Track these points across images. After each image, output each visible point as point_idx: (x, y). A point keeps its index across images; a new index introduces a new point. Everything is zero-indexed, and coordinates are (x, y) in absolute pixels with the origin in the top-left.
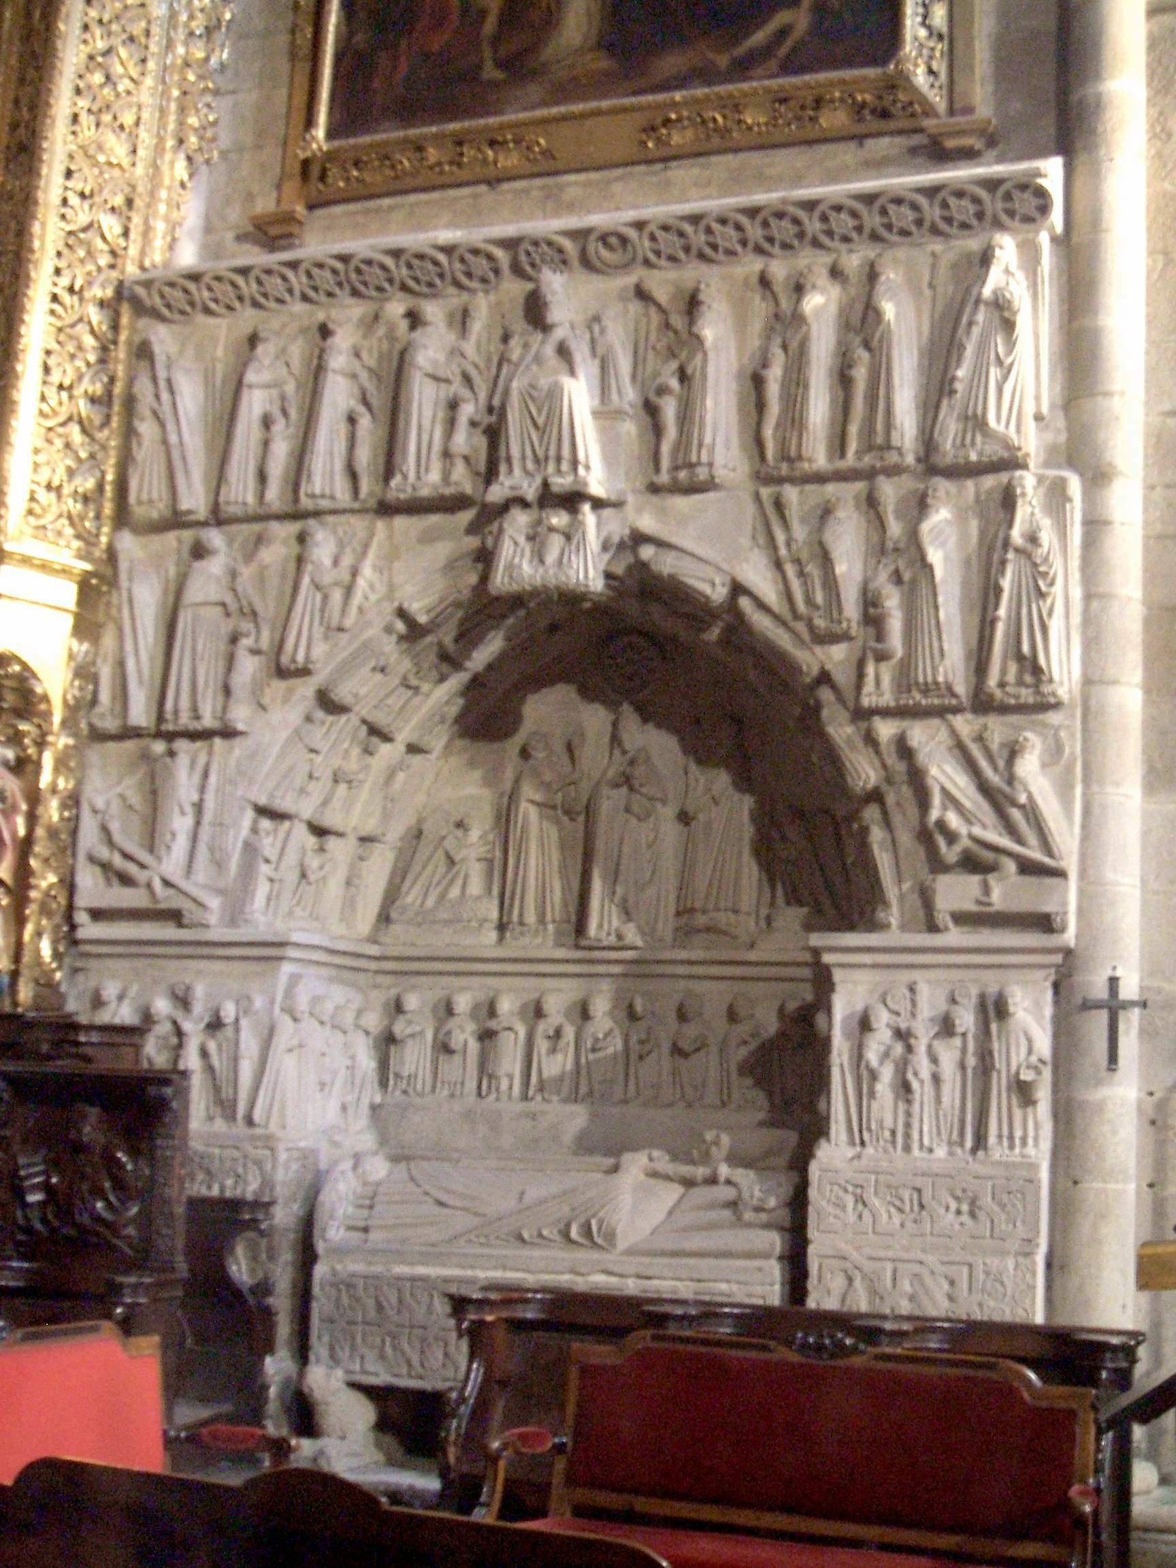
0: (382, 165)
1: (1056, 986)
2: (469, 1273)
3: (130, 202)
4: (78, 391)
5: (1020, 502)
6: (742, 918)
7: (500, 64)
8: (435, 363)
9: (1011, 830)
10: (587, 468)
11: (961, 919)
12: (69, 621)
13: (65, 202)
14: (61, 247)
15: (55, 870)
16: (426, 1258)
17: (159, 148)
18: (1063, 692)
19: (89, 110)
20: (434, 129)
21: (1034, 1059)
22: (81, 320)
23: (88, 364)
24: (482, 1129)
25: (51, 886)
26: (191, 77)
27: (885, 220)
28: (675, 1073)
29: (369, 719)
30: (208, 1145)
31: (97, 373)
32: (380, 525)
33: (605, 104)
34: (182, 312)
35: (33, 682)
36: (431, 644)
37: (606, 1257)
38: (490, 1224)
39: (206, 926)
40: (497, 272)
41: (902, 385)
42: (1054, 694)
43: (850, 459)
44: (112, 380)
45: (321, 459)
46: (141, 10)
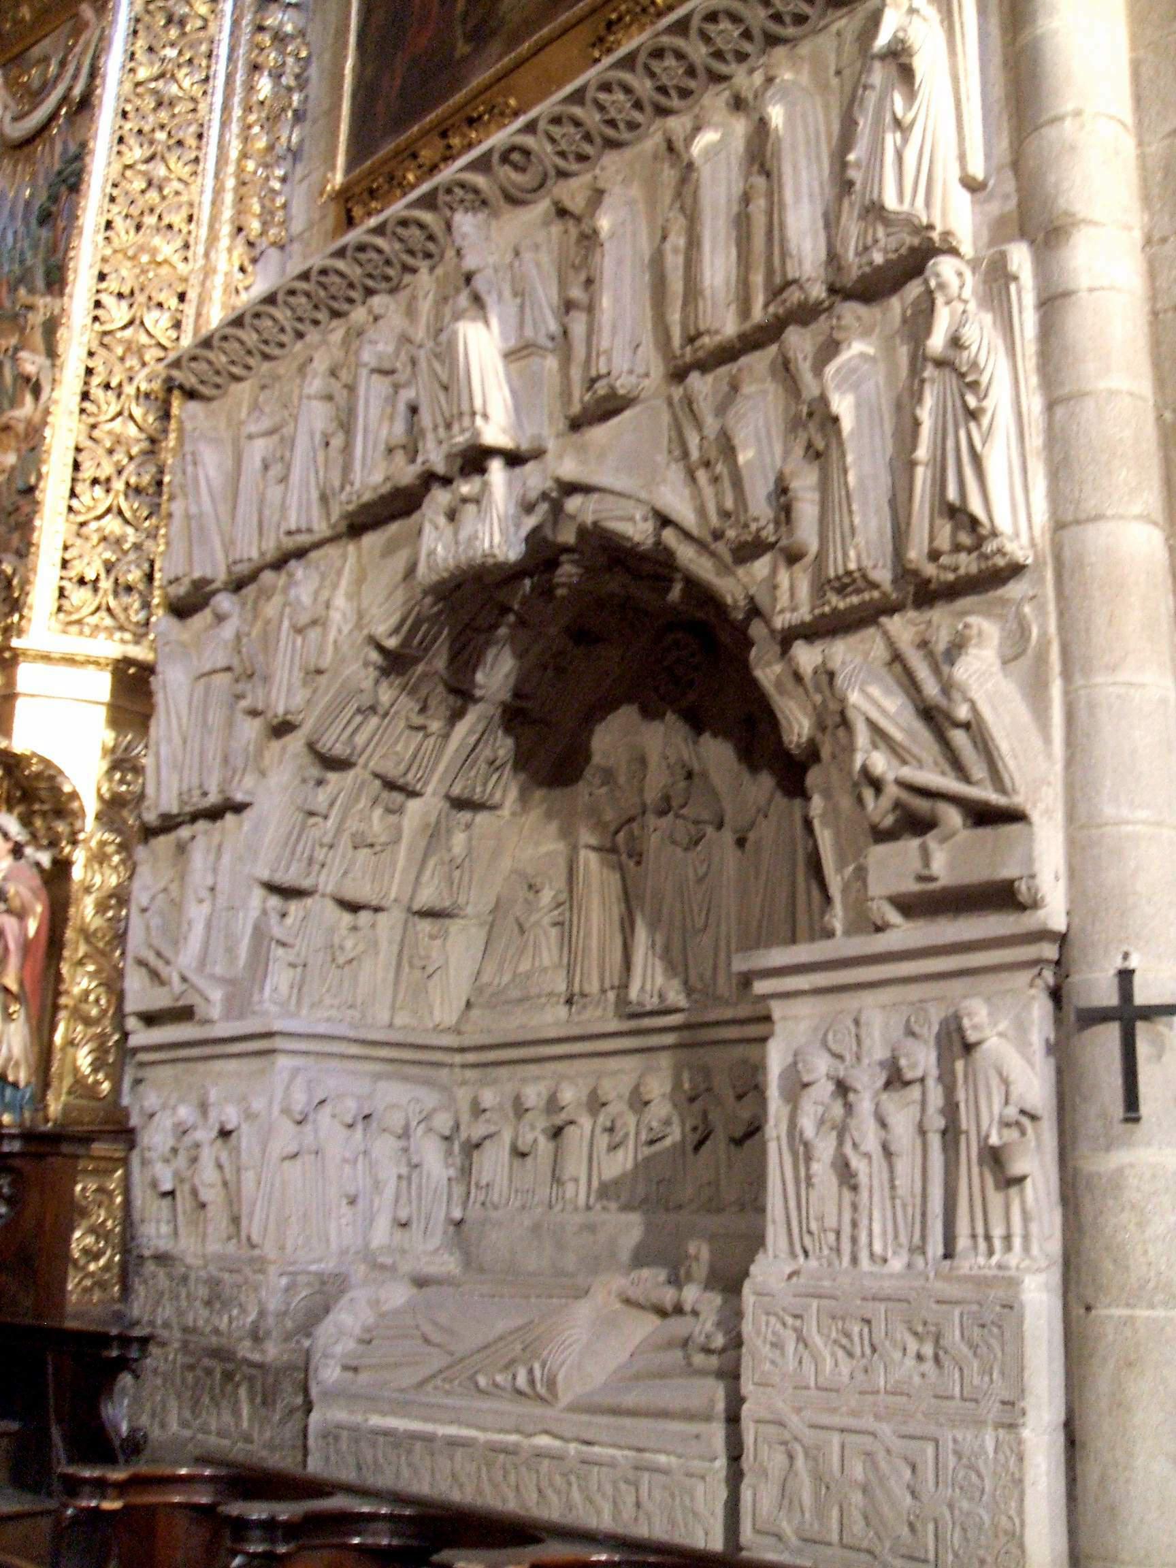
0: (391, 187)
1: (1056, 995)
2: (429, 1427)
3: (182, 297)
4: (118, 485)
5: (940, 300)
7: (469, 38)
8: (380, 357)
9: (958, 768)
10: (485, 416)
11: (910, 907)
12: (102, 713)
13: (98, 304)
14: (95, 346)
15: (92, 976)
16: (401, 1407)
17: (213, 239)
18: (1019, 550)
19: (127, 216)
20: (415, 128)
21: (1012, 1112)
22: (120, 414)
23: (131, 458)
25: (87, 993)
26: (250, 165)
27: (771, 12)
29: (379, 770)
30: (221, 1270)
31: (140, 465)
32: (351, 548)
33: (545, 31)
34: (218, 386)
35: (59, 779)
36: (425, 675)
37: (550, 1412)
40: (431, 238)
41: (797, 199)
42: (1000, 551)
43: (758, 314)
44: (161, 471)
46: (190, 116)
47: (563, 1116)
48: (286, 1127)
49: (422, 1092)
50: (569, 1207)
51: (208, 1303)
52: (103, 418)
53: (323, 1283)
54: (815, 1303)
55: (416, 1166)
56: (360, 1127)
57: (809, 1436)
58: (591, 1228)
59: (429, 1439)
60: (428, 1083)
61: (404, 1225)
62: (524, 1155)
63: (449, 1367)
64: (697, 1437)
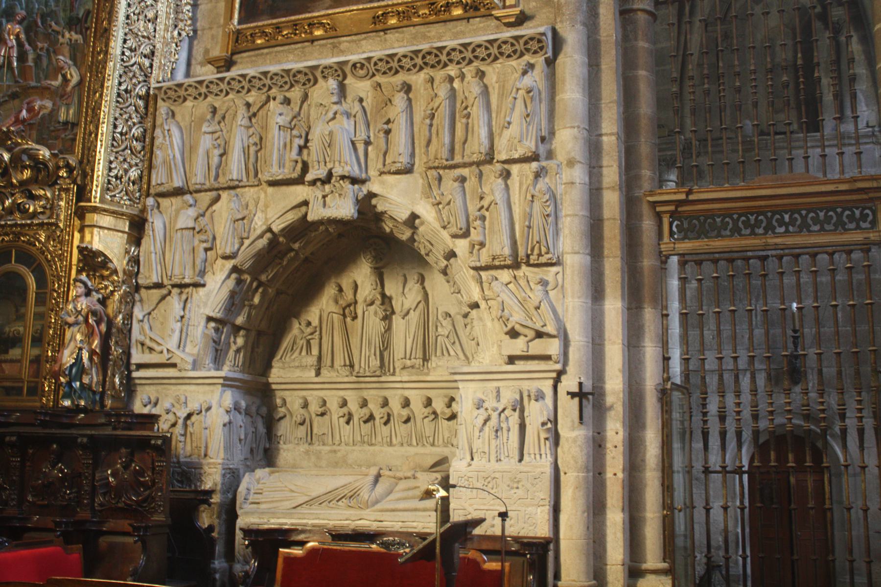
3: (153, 53)
16: (286, 515)
24: (313, 458)
45: (236, 164)
52: (124, 106)
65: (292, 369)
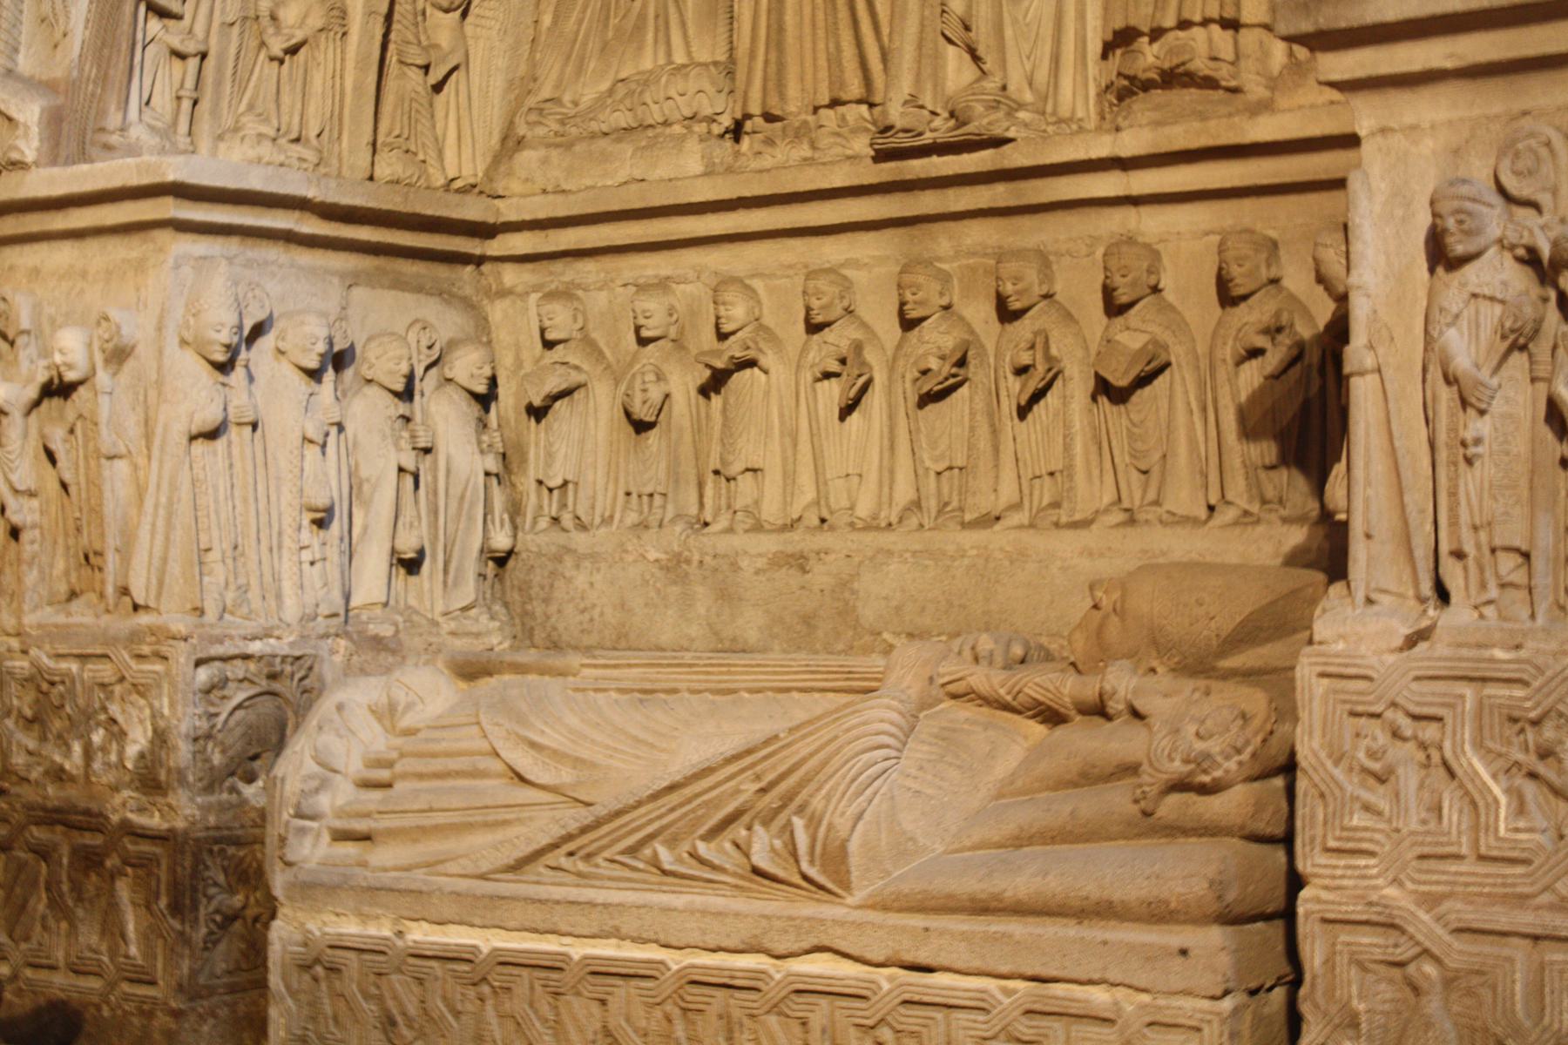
2: (549, 944)
6: (1248, 38)
28: (1100, 441)
30: (60, 656)
37: (829, 911)
38: (598, 824)
39: (18, 165)
47: (733, 348)
48: (191, 374)
49: (429, 309)
50: (743, 521)
51: (34, 722)
53: (273, 676)
54: (1468, 691)
55: (427, 451)
56: (329, 375)
57: (1460, 952)
58: (799, 562)
59: (552, 966)
60: (444, 294)
61: (412, 565)
62: (641, 427)
63: (584, 830)
64: (1184, 952)
65: (603, 143)
